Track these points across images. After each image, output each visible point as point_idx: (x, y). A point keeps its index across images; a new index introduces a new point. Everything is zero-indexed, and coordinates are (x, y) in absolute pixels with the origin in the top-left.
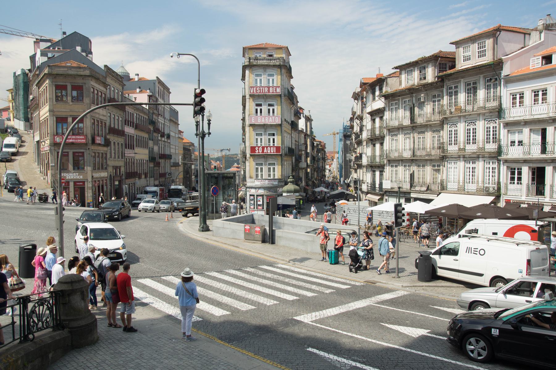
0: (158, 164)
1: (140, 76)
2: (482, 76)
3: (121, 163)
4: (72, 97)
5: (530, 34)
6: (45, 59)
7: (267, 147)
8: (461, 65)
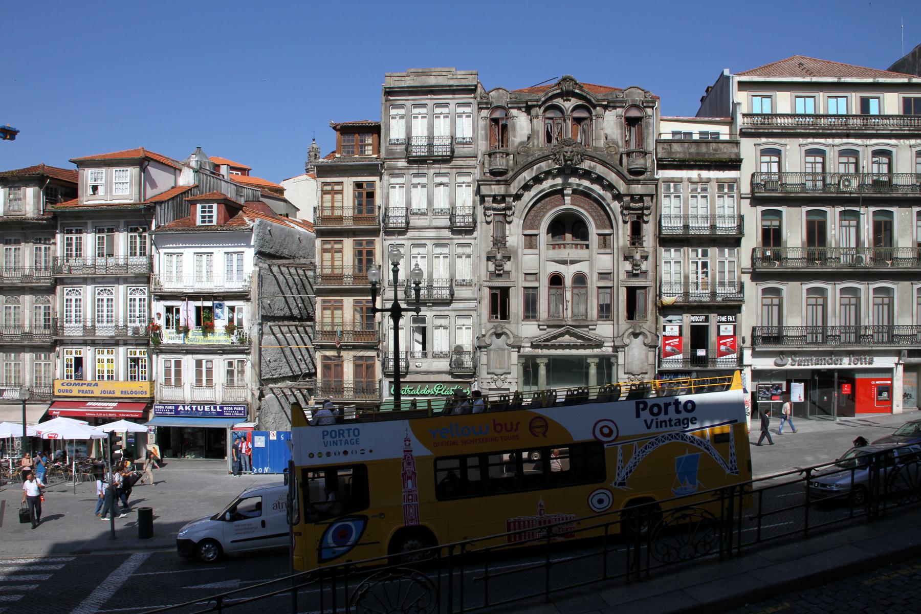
2: (122, 221)
5: (181, 170)
8: (86, 199)
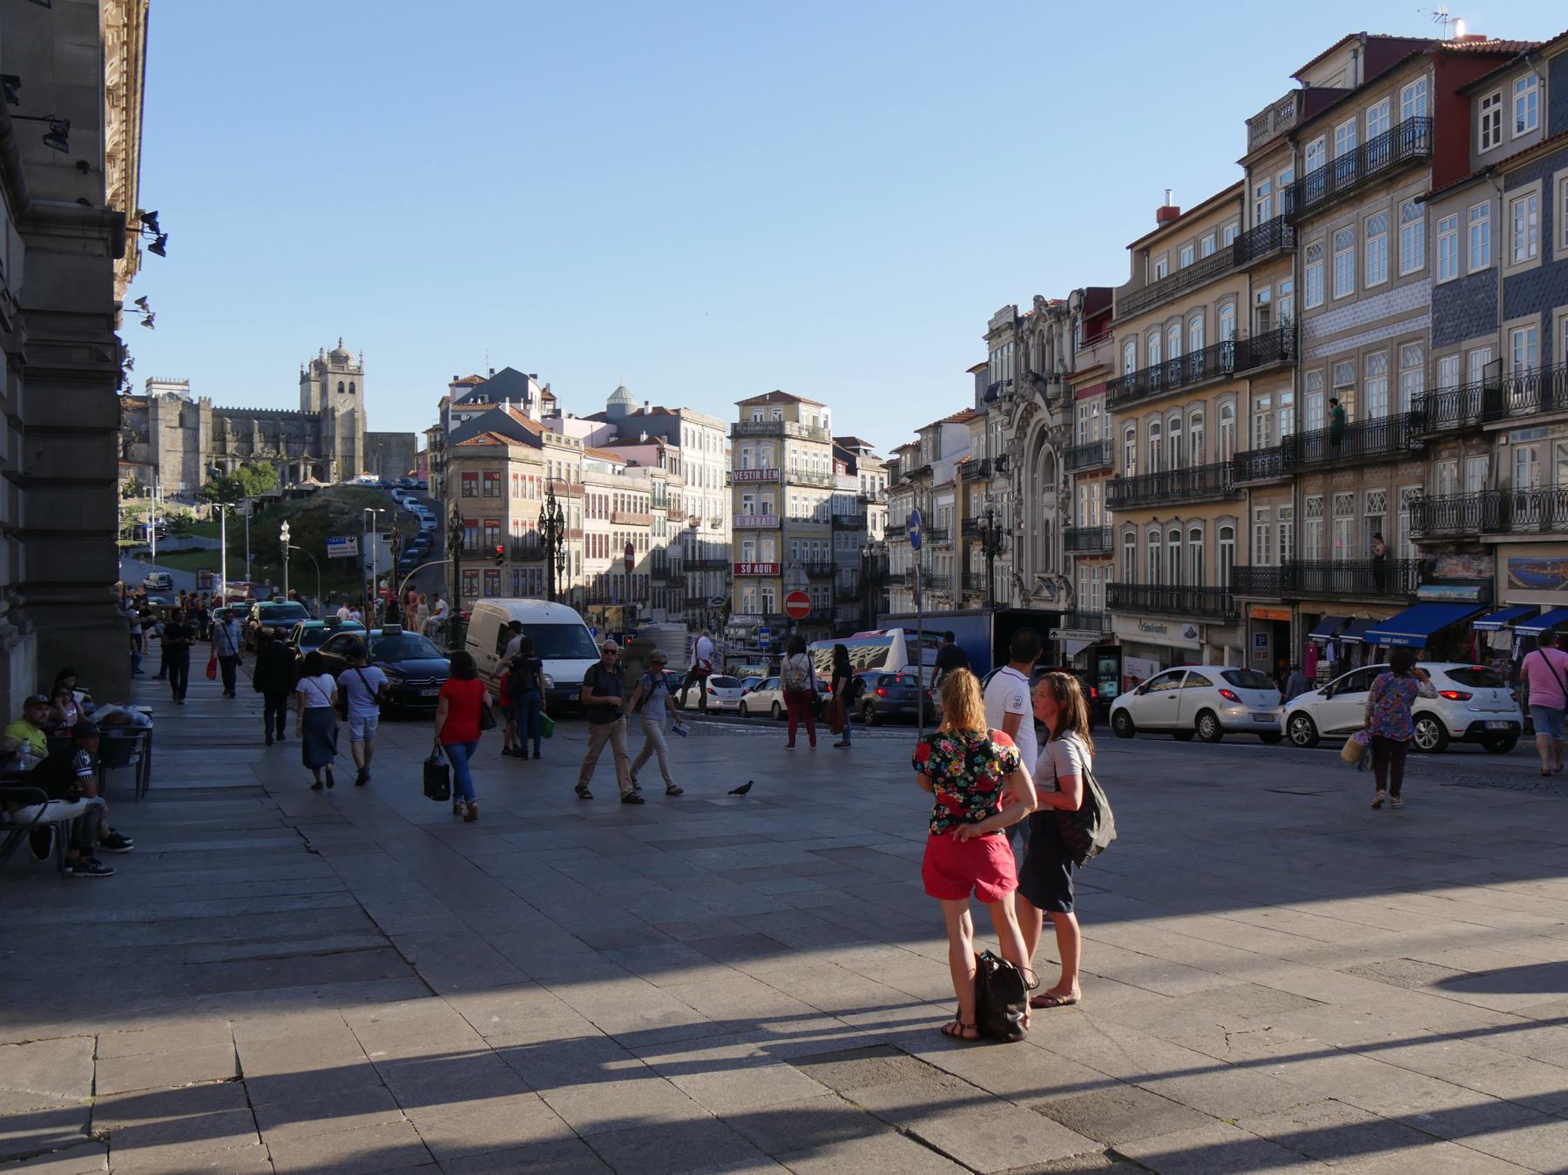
0: (681, 582)
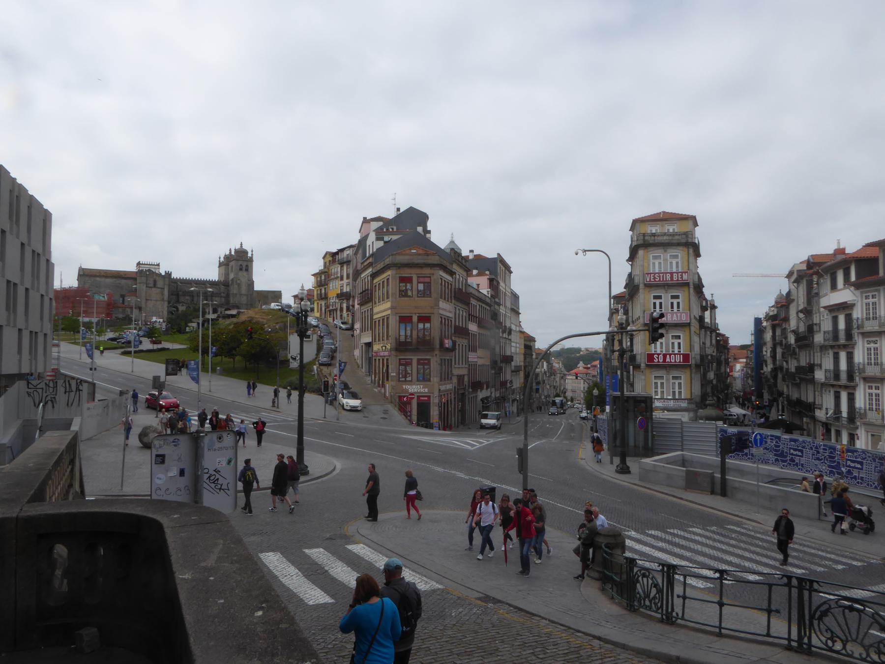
1: (475, 253)
3: (464, 372)
4: (418, 291)
6: (381, 244)
7: (670, 355)
